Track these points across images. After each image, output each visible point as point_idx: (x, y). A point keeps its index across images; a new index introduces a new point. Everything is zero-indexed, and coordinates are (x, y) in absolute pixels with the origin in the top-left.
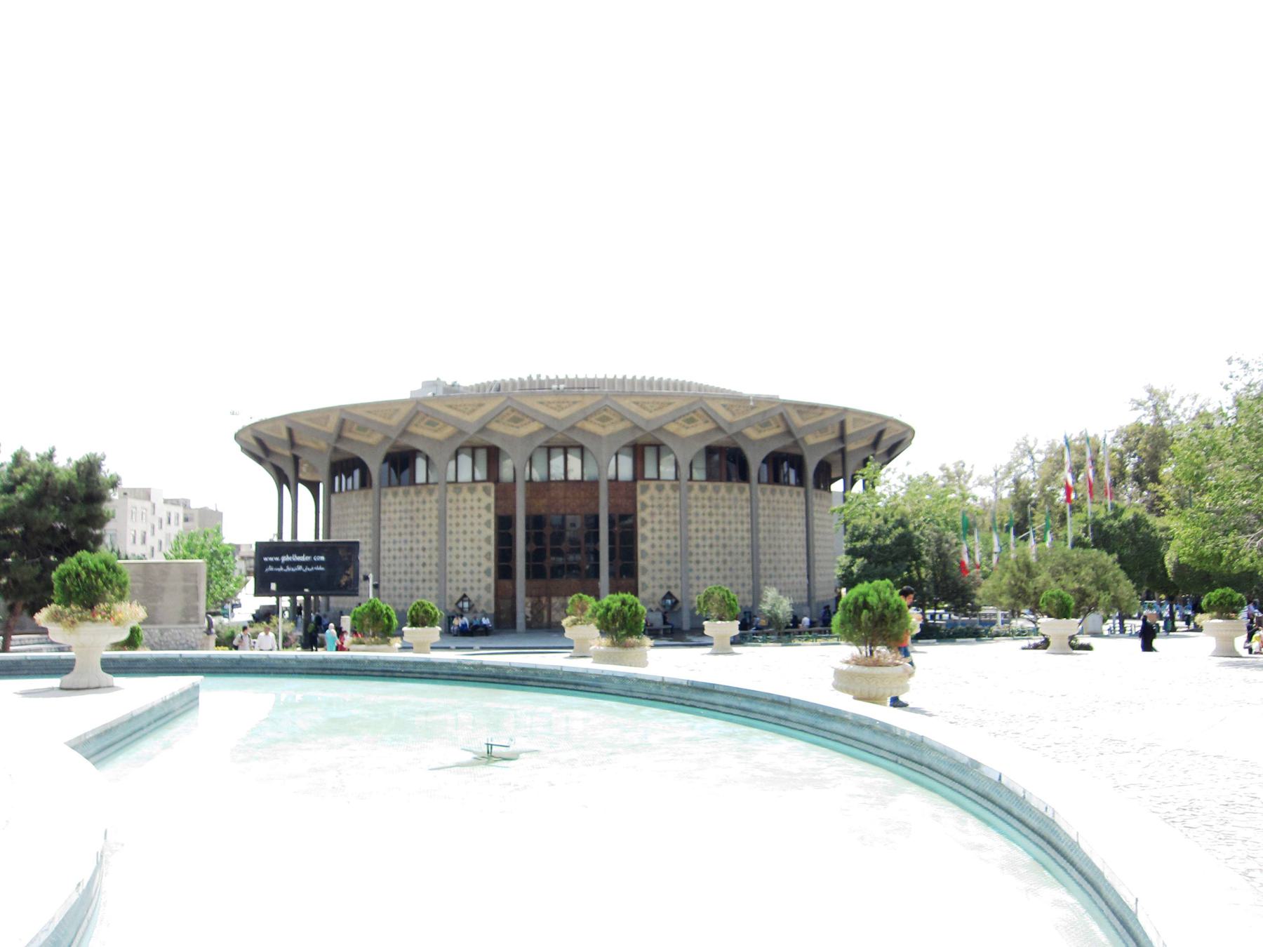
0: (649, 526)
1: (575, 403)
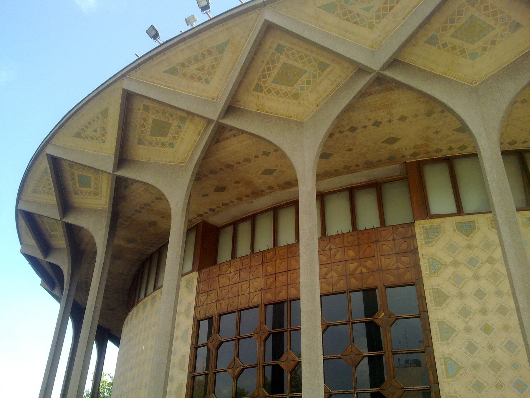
0: (455, 304)
1: (221, 49)
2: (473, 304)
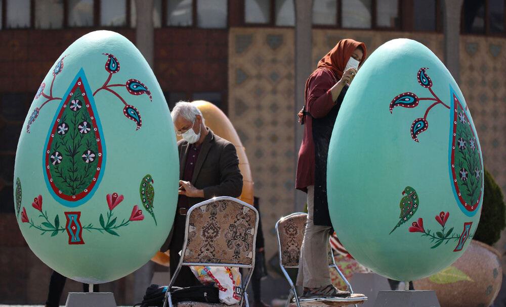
2: (267, 116)
